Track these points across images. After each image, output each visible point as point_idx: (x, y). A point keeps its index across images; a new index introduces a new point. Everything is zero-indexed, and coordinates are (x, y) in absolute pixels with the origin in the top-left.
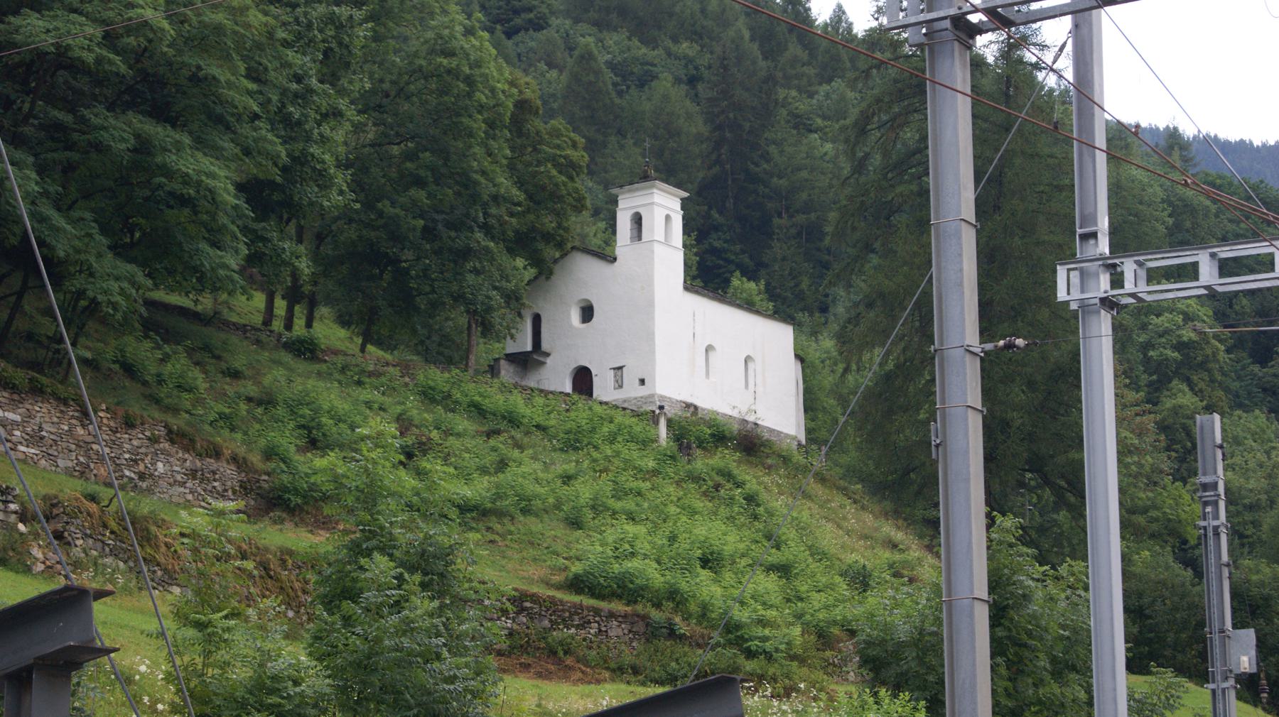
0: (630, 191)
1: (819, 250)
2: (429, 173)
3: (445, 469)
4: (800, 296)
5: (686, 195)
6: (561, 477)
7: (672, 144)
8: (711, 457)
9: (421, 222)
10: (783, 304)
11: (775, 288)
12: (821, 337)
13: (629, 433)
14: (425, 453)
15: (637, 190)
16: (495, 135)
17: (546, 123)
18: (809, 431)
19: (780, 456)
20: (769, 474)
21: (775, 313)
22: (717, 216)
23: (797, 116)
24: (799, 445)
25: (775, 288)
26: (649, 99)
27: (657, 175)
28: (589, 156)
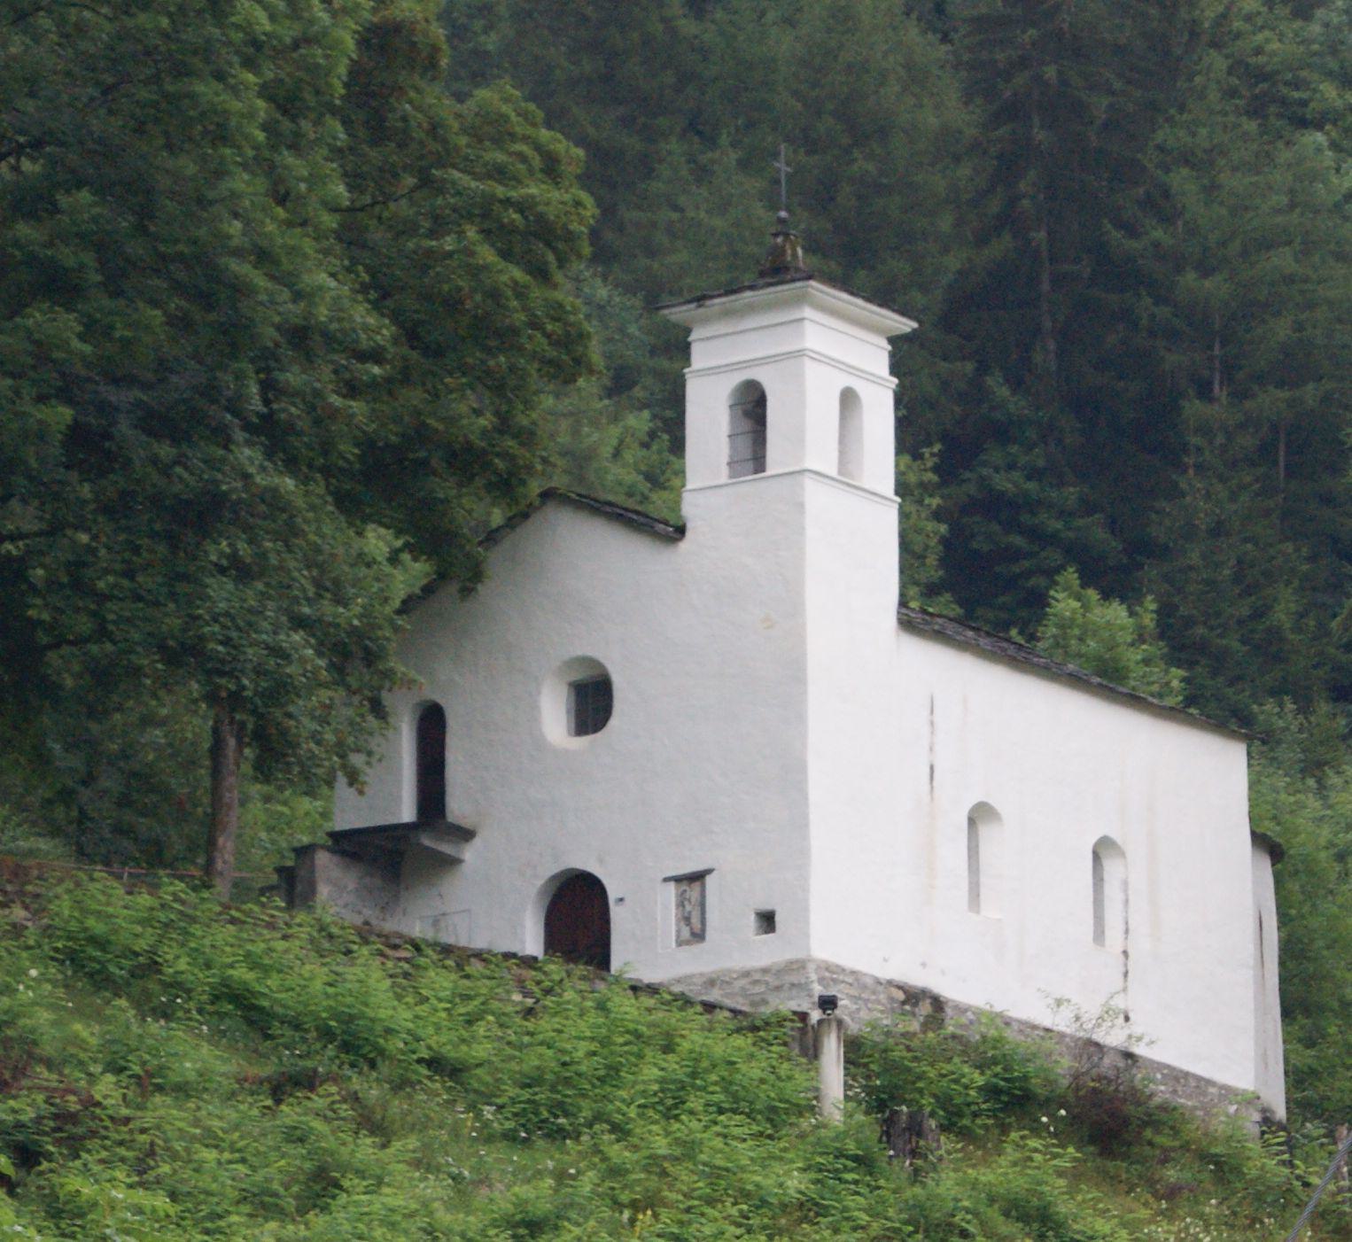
0: (728, 314)
1: (1327, 500)
2: (89, 258)
3: (140, 1197)
4: (1270, 649)
5: (906, 325)
6: (509, 1223)
7: (862, 165)
8: (985, 1161)
9: (63, 414)
10: (1214, 674)
11: (1189, 622)
12: (1334, 780)
13: (726, 1084)
14: (74, 1147)
15: (752, 309)
16: (298, 135)
17: (460, 97)
18: (1297, 1078)
19: (1204, 1157)
20: (1169, 1215)
21: (1190, 701)
22: (1004, 392)
23: (1262, 76)
24: (1267, 1121)
25: (1189, 622)
26: (790, 22)
27: (815, 261)
28: (599, 202)
